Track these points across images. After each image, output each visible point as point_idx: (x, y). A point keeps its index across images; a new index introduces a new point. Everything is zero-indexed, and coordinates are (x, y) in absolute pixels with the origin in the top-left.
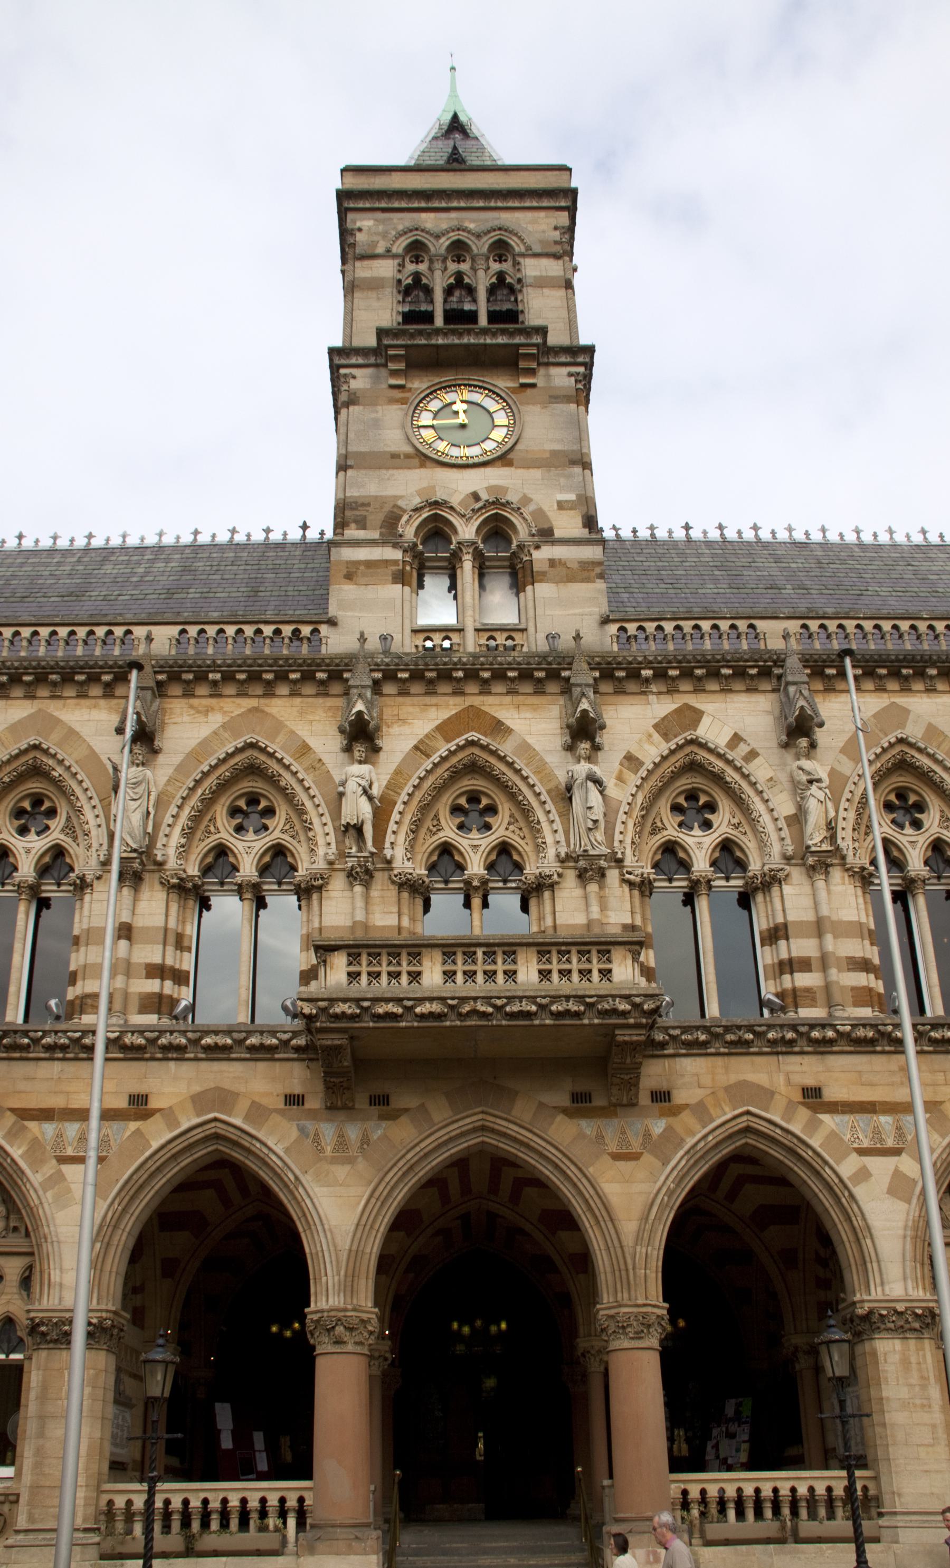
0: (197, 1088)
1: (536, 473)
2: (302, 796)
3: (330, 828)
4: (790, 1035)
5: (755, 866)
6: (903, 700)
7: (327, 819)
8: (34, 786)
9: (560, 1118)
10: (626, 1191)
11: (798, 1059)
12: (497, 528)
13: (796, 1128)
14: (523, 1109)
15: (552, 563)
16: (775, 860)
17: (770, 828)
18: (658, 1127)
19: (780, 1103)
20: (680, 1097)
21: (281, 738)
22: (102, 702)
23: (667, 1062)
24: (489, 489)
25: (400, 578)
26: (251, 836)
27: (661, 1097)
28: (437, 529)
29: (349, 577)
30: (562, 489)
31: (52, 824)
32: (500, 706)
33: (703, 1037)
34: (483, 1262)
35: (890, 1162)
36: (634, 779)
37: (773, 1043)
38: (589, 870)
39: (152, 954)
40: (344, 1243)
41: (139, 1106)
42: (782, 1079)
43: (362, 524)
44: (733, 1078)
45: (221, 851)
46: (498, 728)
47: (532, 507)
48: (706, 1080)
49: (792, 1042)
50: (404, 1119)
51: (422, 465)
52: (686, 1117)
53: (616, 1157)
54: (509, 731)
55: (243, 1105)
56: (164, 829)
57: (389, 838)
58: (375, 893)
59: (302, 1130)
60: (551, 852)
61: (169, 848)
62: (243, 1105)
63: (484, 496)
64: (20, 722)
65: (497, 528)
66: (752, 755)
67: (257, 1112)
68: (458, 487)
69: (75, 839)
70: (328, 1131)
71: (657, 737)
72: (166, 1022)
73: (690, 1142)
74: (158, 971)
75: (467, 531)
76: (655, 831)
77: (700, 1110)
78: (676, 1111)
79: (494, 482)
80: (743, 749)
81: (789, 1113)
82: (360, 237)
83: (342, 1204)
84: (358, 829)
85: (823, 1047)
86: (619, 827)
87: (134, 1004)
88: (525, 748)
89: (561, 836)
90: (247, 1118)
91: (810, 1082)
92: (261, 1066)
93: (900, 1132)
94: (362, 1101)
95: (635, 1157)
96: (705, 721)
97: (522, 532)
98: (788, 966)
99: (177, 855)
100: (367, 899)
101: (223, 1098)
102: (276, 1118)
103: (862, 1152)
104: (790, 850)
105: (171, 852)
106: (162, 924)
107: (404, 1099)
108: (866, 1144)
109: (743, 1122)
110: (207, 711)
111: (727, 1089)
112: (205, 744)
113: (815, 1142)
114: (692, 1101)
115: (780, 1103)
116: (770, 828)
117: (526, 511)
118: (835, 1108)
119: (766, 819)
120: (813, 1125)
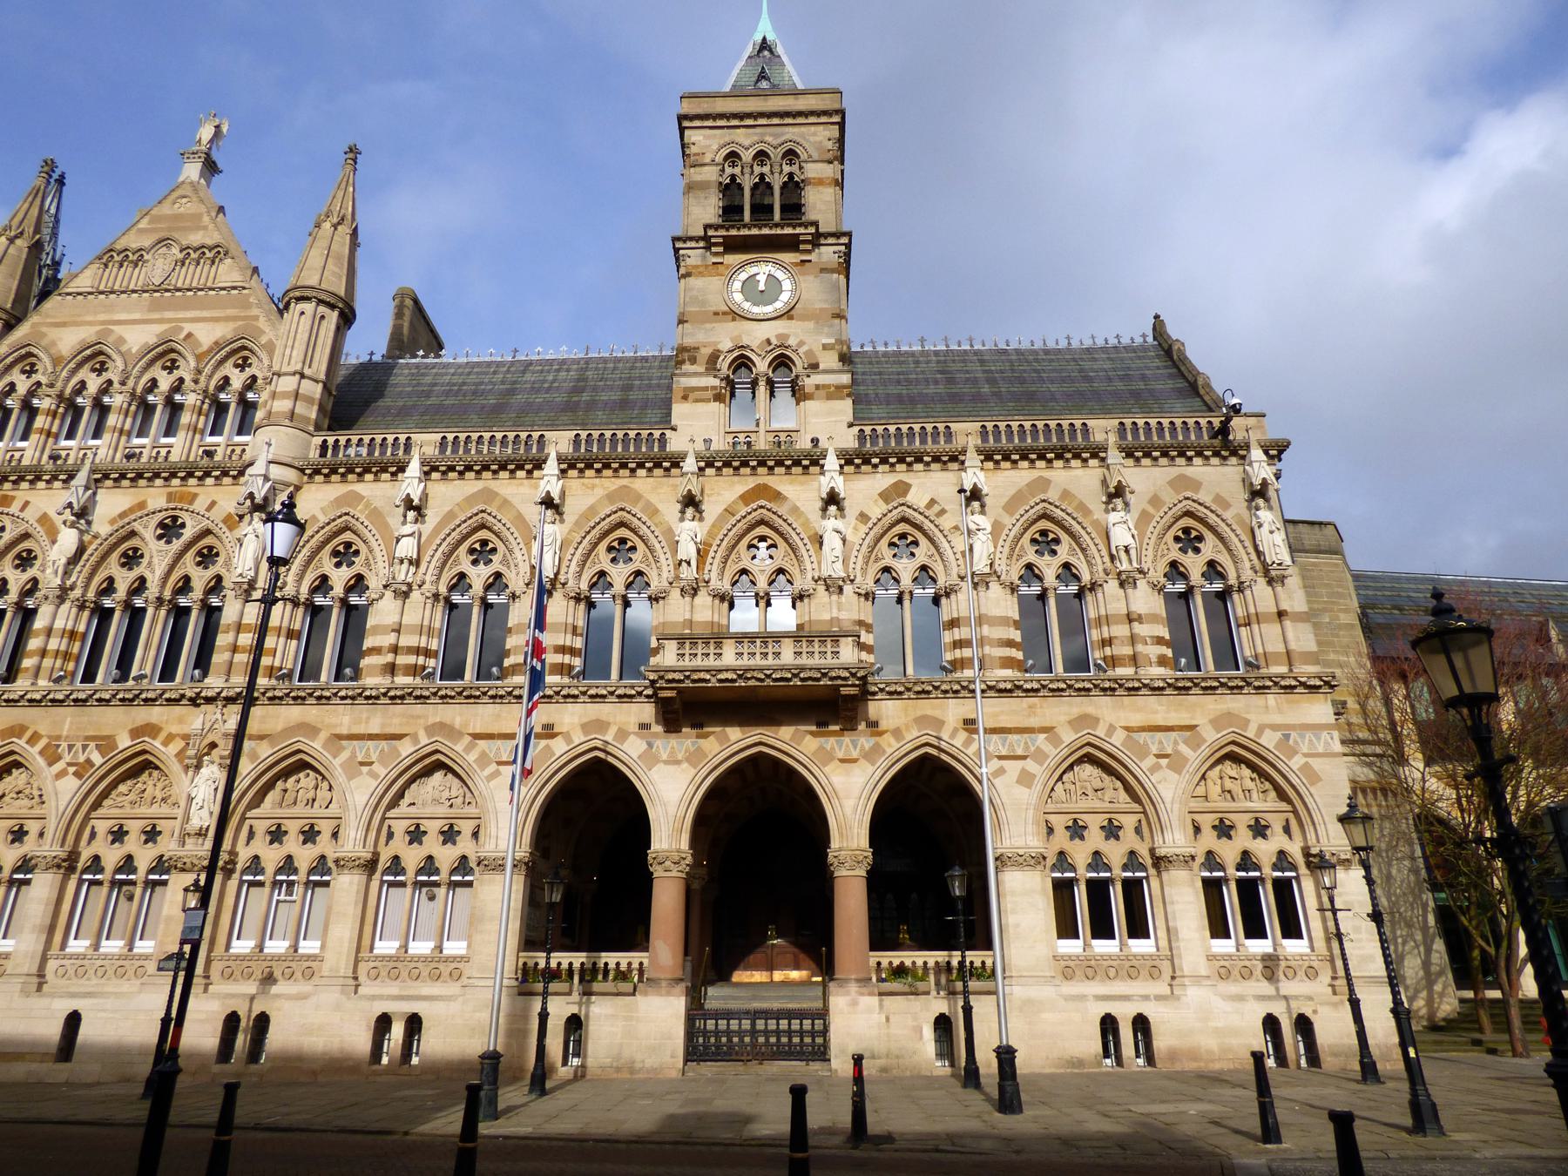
0: (585, 720)
1: (810, 325)
2: (653, 541)
3: (670, 562)
4: (956, 687)
5: (941, 582)
6: (1047, 474)
7: (669, 555)
9: (809, 737)
10: (847, 785)
12: (782, 362)
15: (817, 387)
16: (954, 580)
17: (952, 557)
20: (883, 725)
21: (640, 505)
24: (778, 336)
25: (718, 398)
28: (742, 362)
29: (685, 398)
30: (828, 336)
32: (778, 481)
34: (760, 825)
35: (1019, 764)
36: (864, 529)
38: (834, 586)
40: (672, 810)
43: (693, 361)
44: (919, 713)
46: (777, 496)
47: (805, 348)
49: (956, 692)
51: (734, 320)
53: (842, 761)
54: (785, 498)
57: (708, 567)
60: (809, 577)
63: (774, 341)
65: (782, 362)
66: (943, 512)
68: (755, 336)
71: (881, 502)
72: (566, 680)
75: (762, 366)
76: (876, 560)
77: (897, 733)
78: (880, 734)
79: (781, 331)
80: (936, 508)
83: (673, 784)
86: (853, 559)
88: (795, 510)
89: (815, 565)
93: (1027, 748)
95: (855, 761)
96: (913, 490)
97: (799, 368)
98: (958, 644)
101: (600, 725)
102: (632, 737)
103: (1000, 758)
104: (963, 573)
105: (570, 575)
108: (1004, 753)
112: (592, 510)
114: (892, 727)
116: (952, 557)
117: (801, 351)
119: (949, 552)
120: (968, 743)
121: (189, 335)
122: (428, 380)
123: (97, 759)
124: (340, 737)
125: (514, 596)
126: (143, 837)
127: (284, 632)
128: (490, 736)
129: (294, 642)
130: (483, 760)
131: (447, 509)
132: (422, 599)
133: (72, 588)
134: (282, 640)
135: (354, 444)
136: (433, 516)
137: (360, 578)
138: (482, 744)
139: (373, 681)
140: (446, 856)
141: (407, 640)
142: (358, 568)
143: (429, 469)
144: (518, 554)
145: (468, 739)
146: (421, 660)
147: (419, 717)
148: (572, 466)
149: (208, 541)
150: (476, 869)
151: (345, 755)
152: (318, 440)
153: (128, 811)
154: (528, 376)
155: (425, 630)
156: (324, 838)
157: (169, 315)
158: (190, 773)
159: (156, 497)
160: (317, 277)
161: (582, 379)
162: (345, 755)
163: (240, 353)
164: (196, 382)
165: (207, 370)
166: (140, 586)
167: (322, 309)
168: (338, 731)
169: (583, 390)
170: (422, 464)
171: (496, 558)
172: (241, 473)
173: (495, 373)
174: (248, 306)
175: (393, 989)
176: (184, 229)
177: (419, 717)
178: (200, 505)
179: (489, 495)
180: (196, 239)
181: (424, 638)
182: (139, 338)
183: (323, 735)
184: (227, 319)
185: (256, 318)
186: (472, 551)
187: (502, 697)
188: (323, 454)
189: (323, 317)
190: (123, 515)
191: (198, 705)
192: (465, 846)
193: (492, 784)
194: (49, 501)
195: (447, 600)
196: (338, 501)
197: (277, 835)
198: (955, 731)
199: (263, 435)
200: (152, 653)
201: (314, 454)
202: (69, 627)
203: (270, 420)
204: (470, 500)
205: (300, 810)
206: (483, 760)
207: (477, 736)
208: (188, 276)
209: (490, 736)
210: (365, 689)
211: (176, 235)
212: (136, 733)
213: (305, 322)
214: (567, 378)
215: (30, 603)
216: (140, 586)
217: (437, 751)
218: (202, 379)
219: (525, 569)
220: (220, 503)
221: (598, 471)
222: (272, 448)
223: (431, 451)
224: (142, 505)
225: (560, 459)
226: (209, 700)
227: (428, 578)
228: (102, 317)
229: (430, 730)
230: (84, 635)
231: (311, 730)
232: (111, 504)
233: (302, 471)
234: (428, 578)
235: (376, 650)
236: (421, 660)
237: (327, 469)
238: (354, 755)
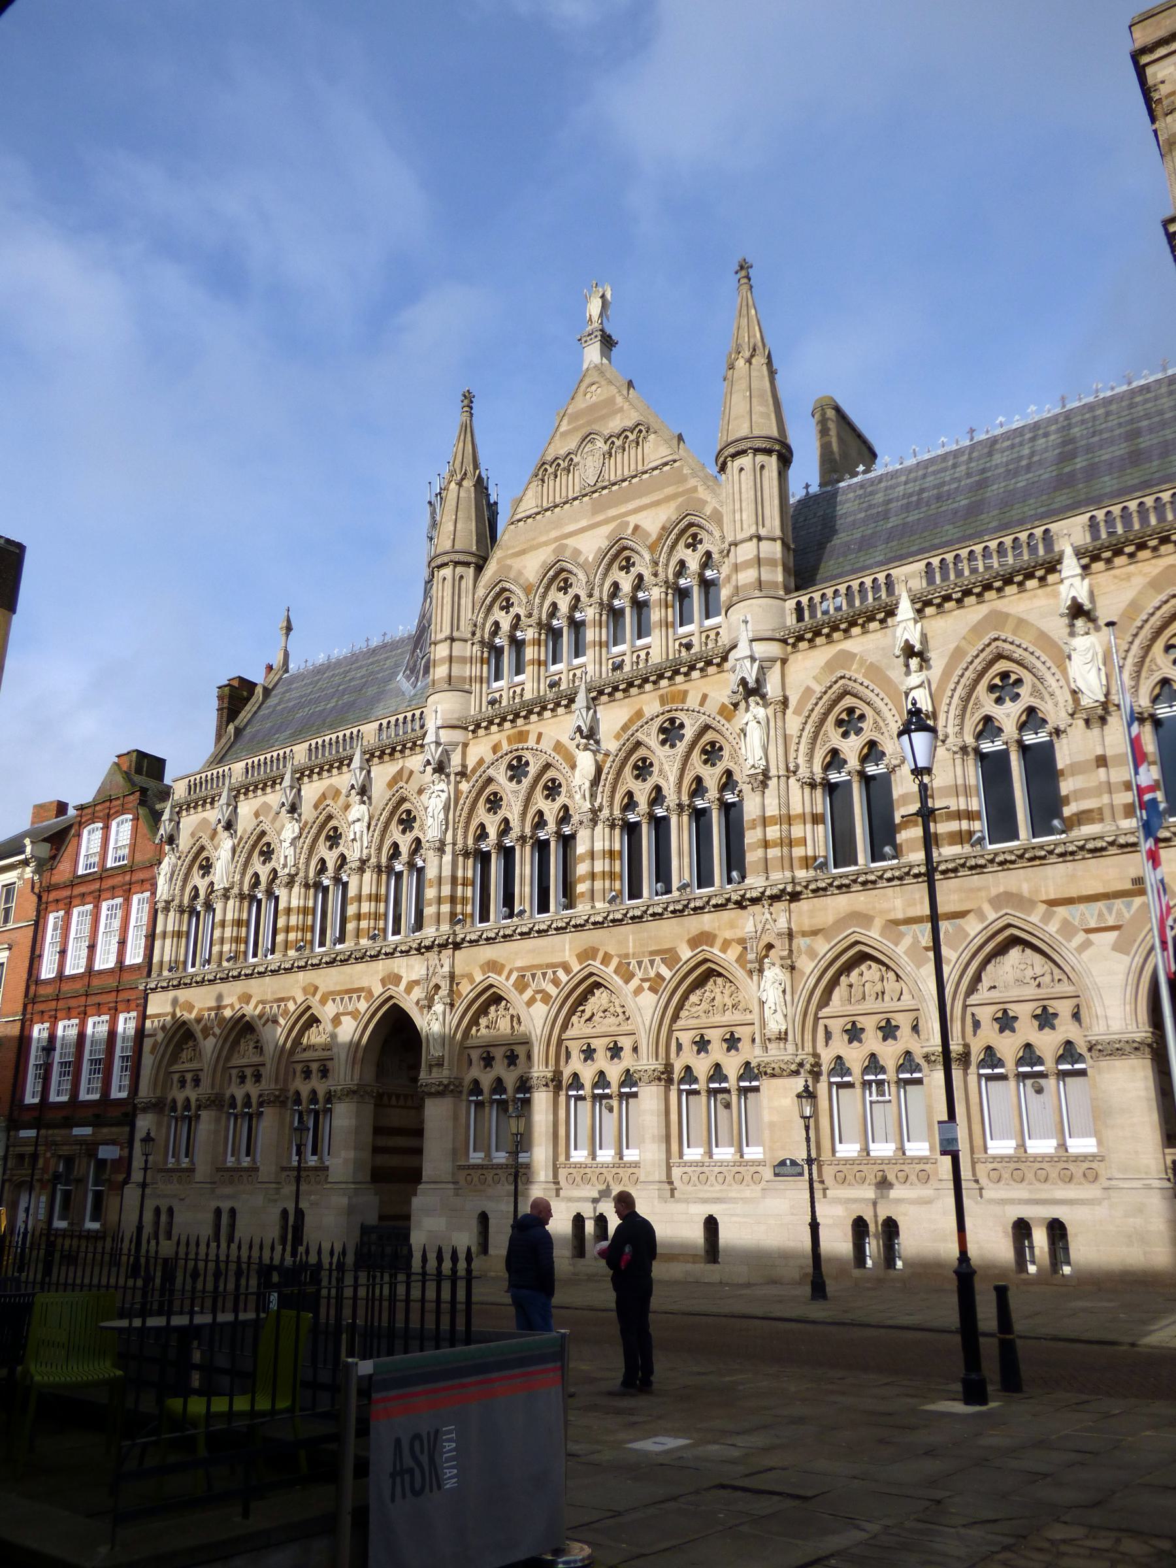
8: (1002, 666)
22: (1040, 591)
31: (1021, 691)
64: (979, 623)
69: (1042, 699)
82: (1164, 90)
110: (1128, 577)
121: (636, 528)
122: (879, 498)
123: (666, 973)
124: (896, 923)
125: (1058, 732)
126: (725, 1046)
127: (808, 818)
128: (1069, 901)
129: (821, 827)
130: (1067, 929)
131: (952, 646)
132: (949, 755)
133: (600, 810)
134: (809, 826)
135: (829, 599)
136: (938, 660)
137: (872, 744)
138: (1061, 911)
140: (1047, 1043)
142: (868, 734)
143: (922, 605)
144: (1051, 681)
145: (1043, 907)
146: (965, 825)
147: (979, 889)
148: (1095, 558)
149: (709, 736)
150: (1087, 1055)
151: (907, 941)
152: (791, 604)
153: (704, 1020)
154: (998, 459)
155: (961, 789)
156: (905, 1032)
157: (612, 512)
158: (755, 978)
159: (650, 703)
160: (746, 425)
161: (1068, 441)
162: (907, 941)
163: (688, 532)
164: (656, 575)
165: (662, 560)
167: (760, 458)
168: (892, 916)
169: (1073, 455)
170: (913, 602)
171: (1023, 691)
172: (725, 659)
173: (954, 466)
174: (683, 479)
175: (1021, 1192)
176: (603, 418)
177: (979, 889)
178: (692, 702)
179: (999, 619)
180: (615, 424)
182: (591, 544)
183: (878, 923)
184: (668, 499)
185: (695, 489)
186: (992, 688)
187: (1072, 853)
188: (800, 618)
189: (762, 467)
191: (745, 908)
192: (1066, 1029)
193: (1085, 955)
194: (558, 729)
195: (977, 751)
196: (830, 666)
197: (854, 1034)
199: (737, 613)
201: (791, 620)
202: (607, 848)
203: (739, 595)
204: (977, 630)
205: (870, 1005)
206: (1067, 929)
207: (1052, 903)
208: (620, 466)
209: (1069, 901)
210: (911, 867)
211: (596, 427)
212: (694, 942)
213: (747, 477)
214: (1048, 444)
215: (567, 830)
217: (1009, 926)
218: (660, 569)
219: (1064, 697)
220: (711, 695)
221: (1131, 555)
222: (748, 623)
223: (919, 585)
224: (639, 714)
225: (1079, 553)
226: (755, 901)
227: (951, 730)
228: (553, 534)
229: (997, 902)
230: (621, 852)
231: (864, 919)
232: (612, 718)
233: (784, 641)
236: (965, 825)
237: (808, 633)
238: (916, 941)
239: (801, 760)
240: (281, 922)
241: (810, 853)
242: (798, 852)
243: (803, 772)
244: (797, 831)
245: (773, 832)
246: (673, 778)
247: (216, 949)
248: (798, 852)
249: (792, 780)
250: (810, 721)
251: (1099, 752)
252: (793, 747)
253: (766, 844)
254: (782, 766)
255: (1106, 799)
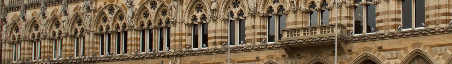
0: (267, 55)
9: (331, 56)
11: (378, 41)
13: (375, 55)
14: (324, 55)
18: (348, 57)
19: (373, 50)
20: (353, 51)
23: (351, 44)
26: (276, 3)
27: (350, 51)
33: (357, 39)
35: (394, 60)
37: (372, 39)
39: (258, 30)
41: (258, 59)
42: (374, 46)
44: (364, 46)
45: (271, 7)
48: (359, 47)
50: (303, 58)
52: (354, 55)
55: (275, 58)
56: (259, 6)
58: (298, 14)
59: (285, 61)
61: (260, 9)
62: (275, 58)
67: (277, 59)
70: (289, 61)
73: (354, 59)
74: (260, 34)
77: (357, 53)
78: (352, 54)
81: (374, 53)
84: (293, 2)
85: (382, 39)
87: (256, 40)
90: (276, 60)
91: (380, 46)
92: (278, 50)
93: (397, 55)
94: (295, 55)
99: (262, 10)
100: (296, 16)
103: (389, 59)
106: (259, 24)
107: (303, 55)
109: (365, 55)
111: (363, 49)
113: (379, 58)
114: (355, 51)
115: (373, 50)
118: (384, 51)
120: (379, 55)
125: (245, 18)
127: (187, 34)
129: (190, 37)
132: (221, 21)
134: (187, 37)
139: (211, 47)
141: (219, 34)
146: (223, 40)
155: (223, 31)
166: (150, 23)
181: (223, 33)
190: (141, 2)
198: (375, 51)
200: (157, 42)
210: (209, 50)
216: (150, 23)
227: (222, 14)
234: (222, 14)
235: (211, 38)
236: (223, 40)
239: (186, 18)
240: (42, 50)
241: (187, 44)
242: (184, 43)
243: (186, 21)
244: (184, 38)
245: (177, 38)
246: (153, 19)
247: (22, 56)
248: (184, 43)
249: (183, 24)
250: (189, 7)
251: (253, 24)
252: (184, 14)
253: (175, 41)
254: (181, 19)
255: (252, 37)
